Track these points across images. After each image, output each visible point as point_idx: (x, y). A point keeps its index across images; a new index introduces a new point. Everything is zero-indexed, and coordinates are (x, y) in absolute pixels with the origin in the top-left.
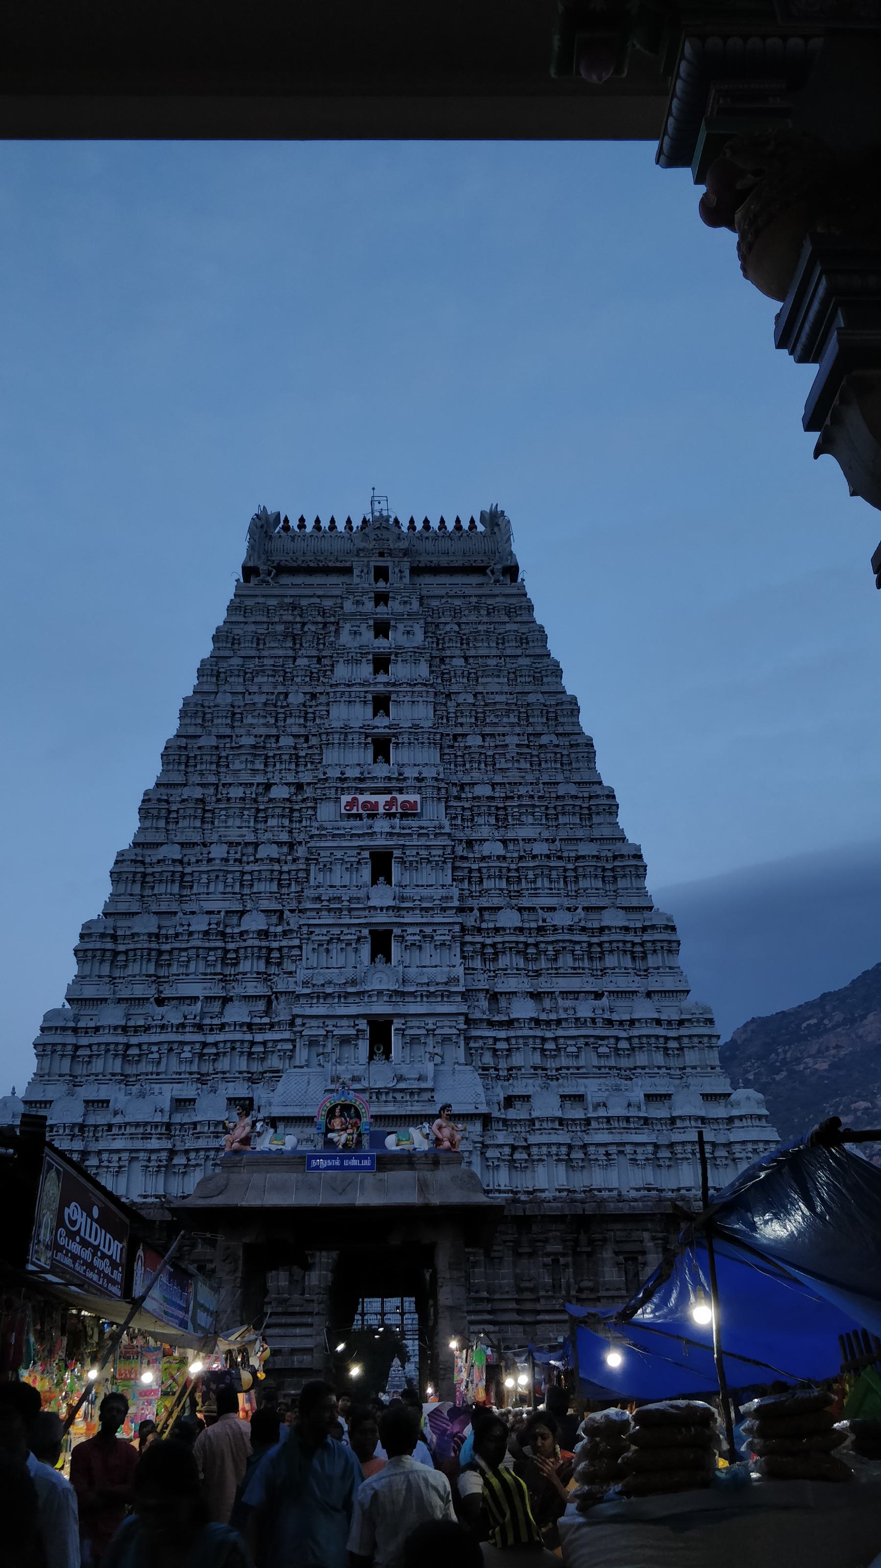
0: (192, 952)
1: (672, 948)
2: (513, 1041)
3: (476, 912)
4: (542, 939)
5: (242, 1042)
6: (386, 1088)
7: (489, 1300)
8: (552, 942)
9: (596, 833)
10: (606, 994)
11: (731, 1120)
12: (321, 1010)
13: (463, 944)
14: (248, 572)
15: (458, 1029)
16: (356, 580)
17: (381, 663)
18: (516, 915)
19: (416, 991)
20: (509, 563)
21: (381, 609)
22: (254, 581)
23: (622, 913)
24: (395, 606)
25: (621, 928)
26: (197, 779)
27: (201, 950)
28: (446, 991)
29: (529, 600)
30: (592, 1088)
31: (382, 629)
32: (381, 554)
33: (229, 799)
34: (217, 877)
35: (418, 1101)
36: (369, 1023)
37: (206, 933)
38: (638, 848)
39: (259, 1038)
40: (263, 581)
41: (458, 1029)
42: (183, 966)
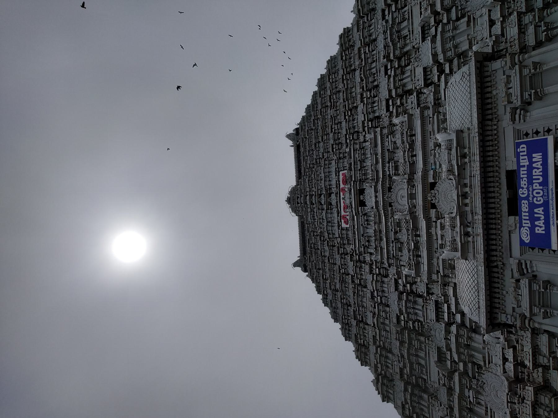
0: (414, 359)
2: (449, 54)
4: (392, 55)
5: (457, 336)
6: (457, 188)
8: (394, 45)
12: (424, 253)
15: (433, 115)
19: (409, 162)
27: (411, 351)
28: (407, 133)
34: (382, 323)
35: (469, 148)
37: (402, 343)
41: (433, 115)
42: (422, 370)
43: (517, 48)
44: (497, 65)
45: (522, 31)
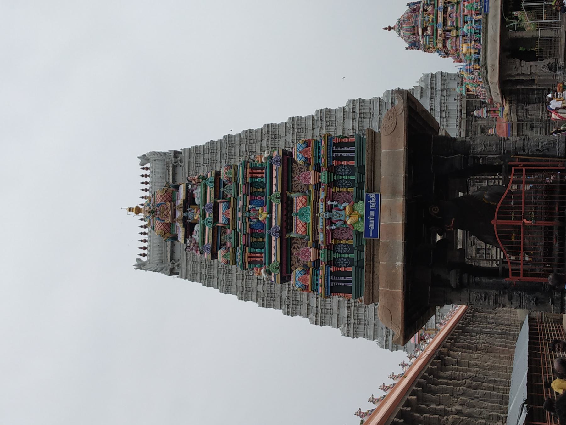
1: (362, 101)
9: (310, 127)
11: (432, 88)
14: (172, 272)
20: (172, 154)
23: (346, 121)
25: (353, 122)
26: (279, 293)
29: (193, 147)
38: (318, 111)
40: (178, 266)
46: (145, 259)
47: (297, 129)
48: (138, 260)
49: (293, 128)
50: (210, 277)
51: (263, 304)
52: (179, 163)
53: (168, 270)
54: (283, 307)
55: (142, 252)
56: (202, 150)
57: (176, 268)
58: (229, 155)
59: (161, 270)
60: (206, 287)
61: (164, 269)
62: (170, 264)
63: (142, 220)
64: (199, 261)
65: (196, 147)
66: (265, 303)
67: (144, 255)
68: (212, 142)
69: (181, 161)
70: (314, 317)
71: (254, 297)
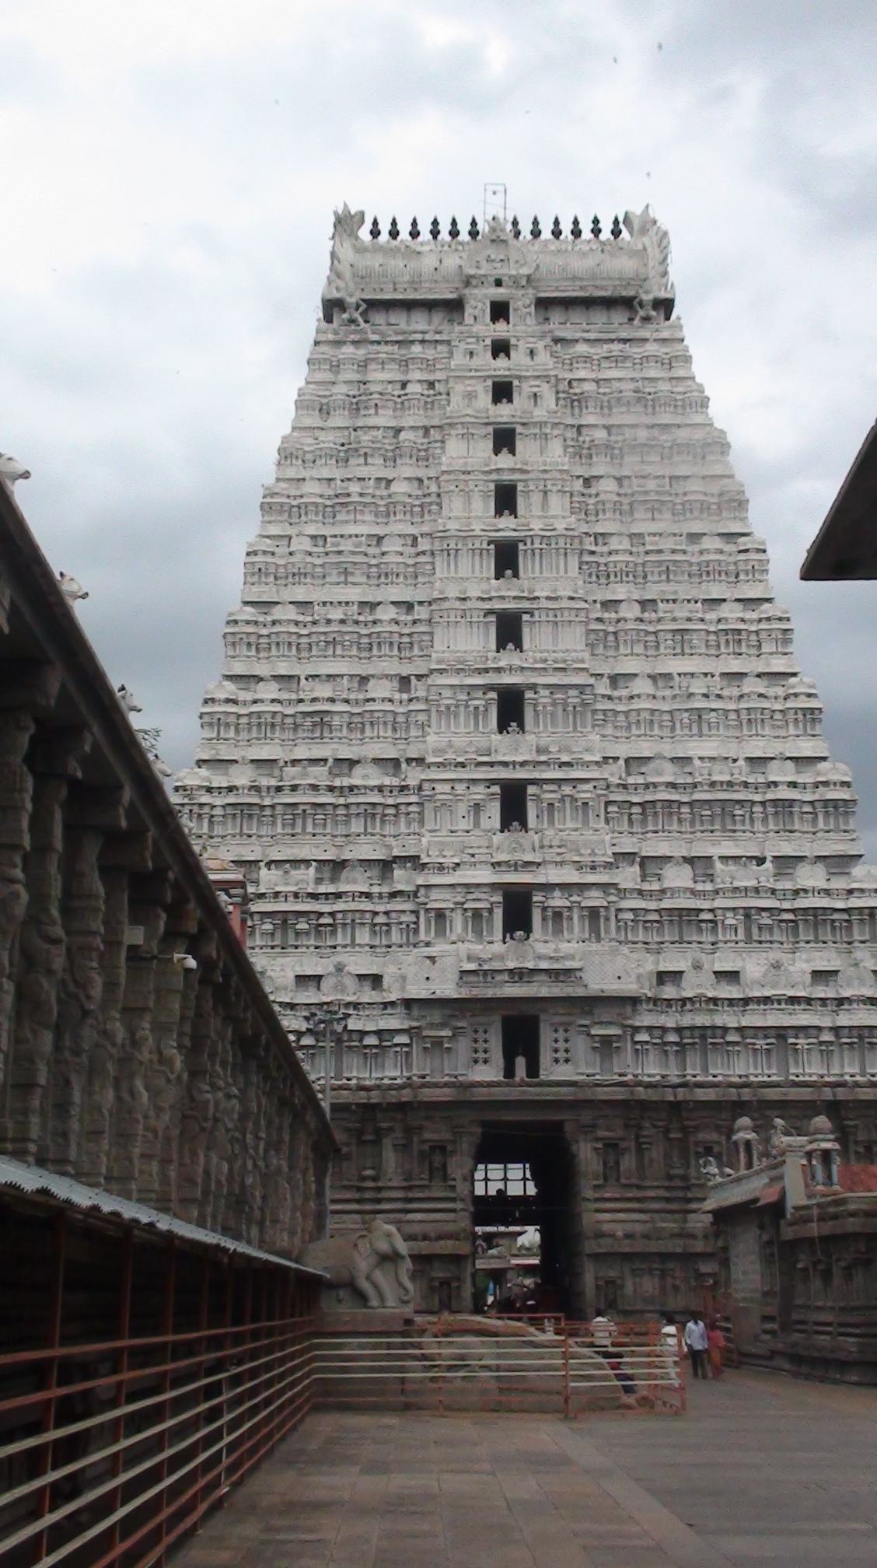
3: (621, 762)
7: (639, 1187)
10: (769, 859)
13: (608, 803)
14: (332, 307)
16: (468, 320)
17: (504, 440)
18: (669, 767)
20: (663, 295)
21: (502, 362)
22: (339, 318)
24: (519, 357)
30: (754, 966)
31: (502, 391)
32: (499, 283)
33: (329, 621)
36: (506, 896)
39: (381, 908)
40: (352, 321)
43: (637, 1024)
44: (629, 1009)
45: (649, 1029)
46: (364, 233)
47: (757, 632)
48: (362, 215)
49: (760, 620)
50: (324, 411)
51: (255, 553)
52: (642, 313)
53: (337, 295)
54: (249, 609)
55: (385, 227)
56: (681, 373)
57: (345, 316)
58: (671, 448)
59: (335, 273)
60: (295, 397)
61: (341, 284)
62: (353, 300)
63: (474, 223)
64: (371, 376)
65: (687, 359)
66: (259, 558)
67: (375, 233)
68: (704, 403)
69: (647, 319)
70: (223, 696)
71: (274, 530)
